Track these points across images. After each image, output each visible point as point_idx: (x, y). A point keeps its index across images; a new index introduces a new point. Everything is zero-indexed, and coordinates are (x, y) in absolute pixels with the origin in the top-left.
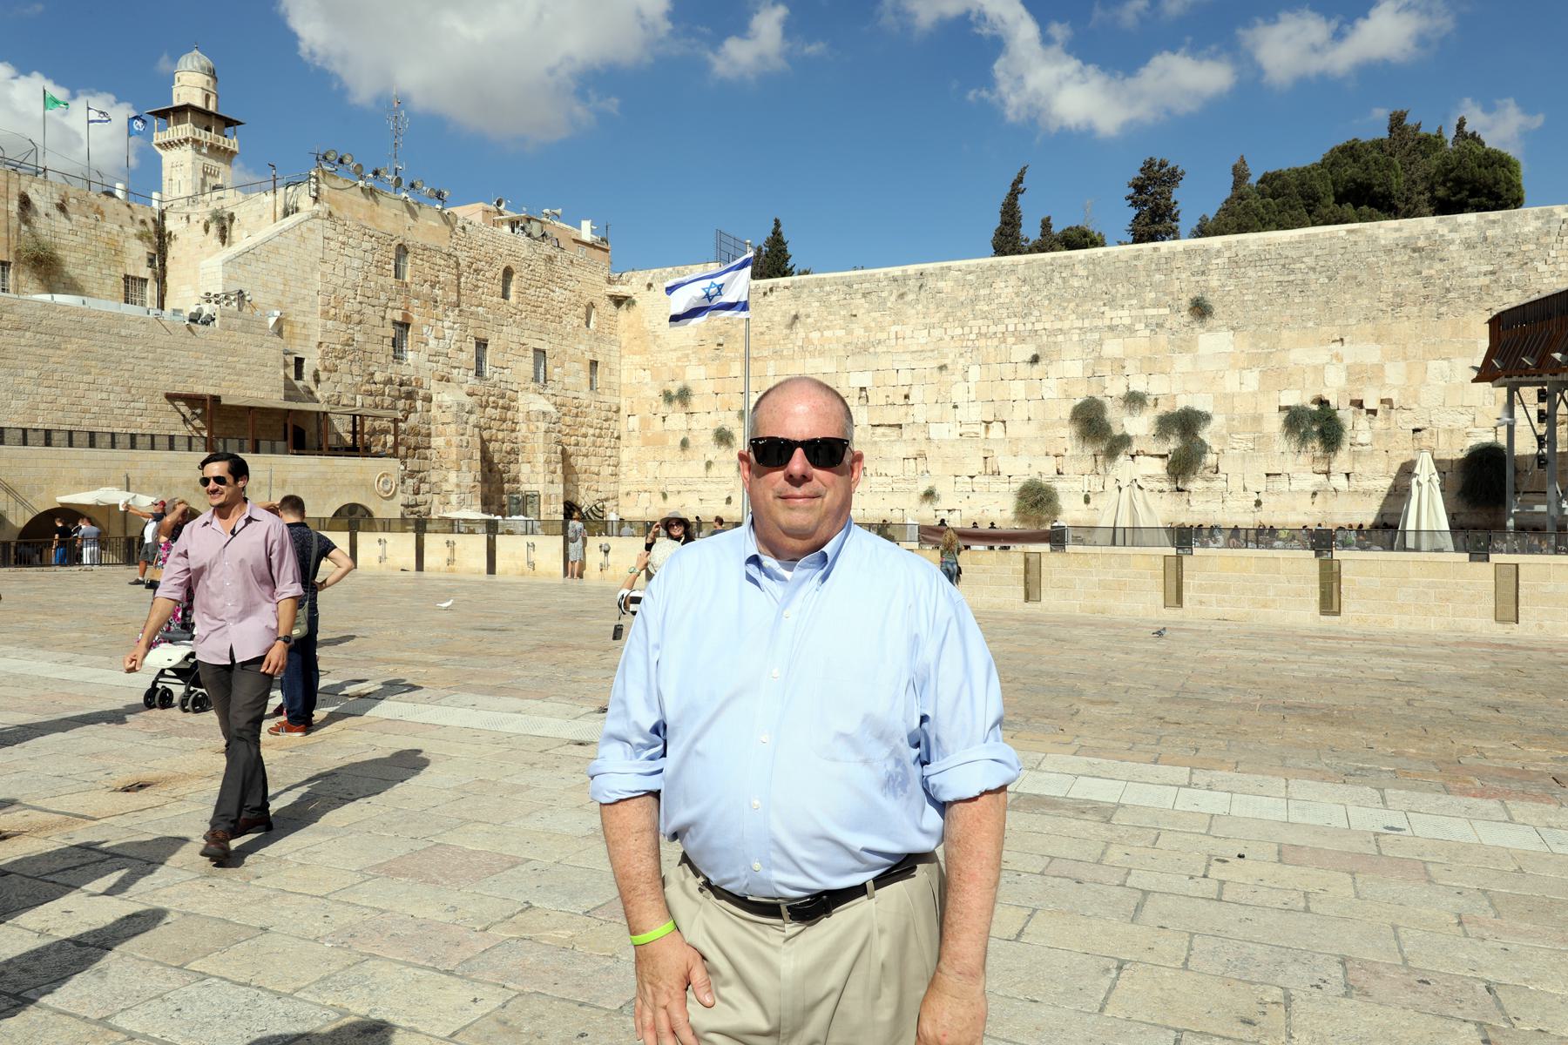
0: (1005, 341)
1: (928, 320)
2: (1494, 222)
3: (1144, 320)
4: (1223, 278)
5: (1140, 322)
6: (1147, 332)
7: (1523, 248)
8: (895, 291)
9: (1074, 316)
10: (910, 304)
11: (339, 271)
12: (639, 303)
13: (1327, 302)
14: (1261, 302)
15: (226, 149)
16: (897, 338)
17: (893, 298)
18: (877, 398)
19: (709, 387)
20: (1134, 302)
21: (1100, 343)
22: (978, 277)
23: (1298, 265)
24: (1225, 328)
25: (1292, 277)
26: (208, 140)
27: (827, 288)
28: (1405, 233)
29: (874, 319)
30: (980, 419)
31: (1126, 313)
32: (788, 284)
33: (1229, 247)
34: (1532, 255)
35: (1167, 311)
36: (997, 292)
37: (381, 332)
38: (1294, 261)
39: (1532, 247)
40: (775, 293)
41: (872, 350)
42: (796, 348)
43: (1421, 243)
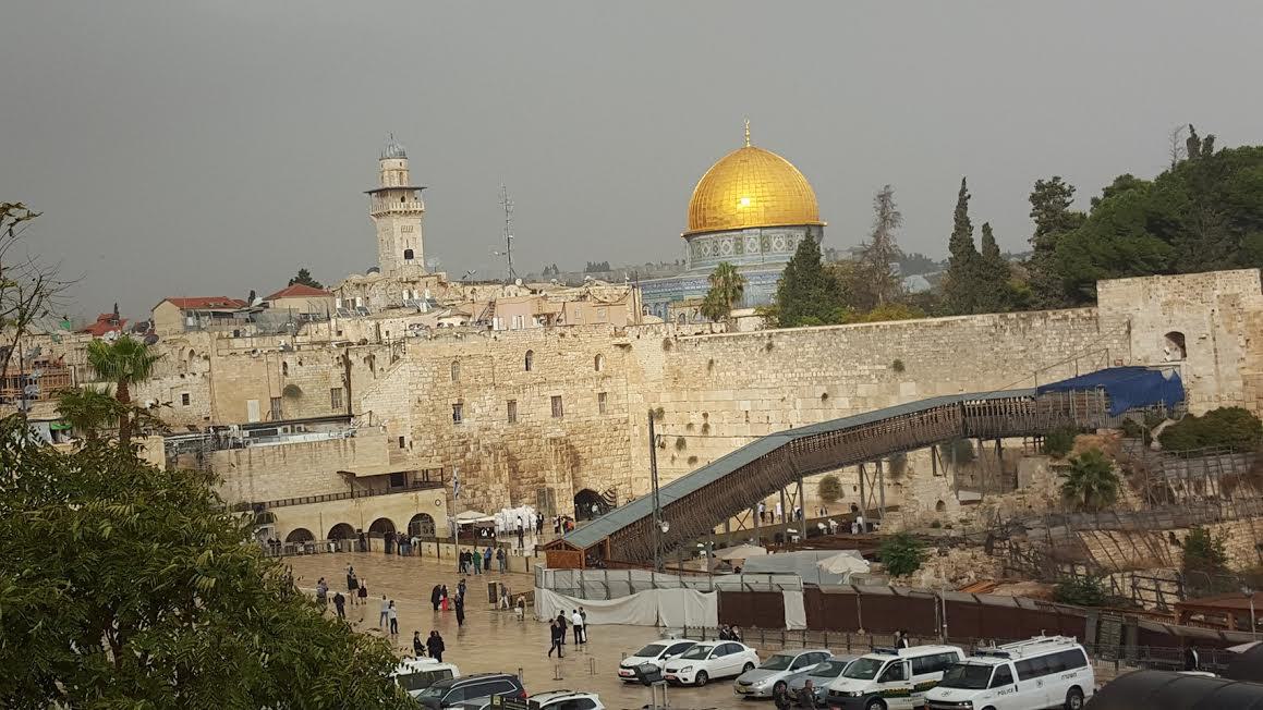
6: (876, 381)
11: (420, 386)
12: (634, 348)
15: (415, 211)
26: (403, 209)
31: (866, 367)
35: (884, 367)
37: (445, 413)
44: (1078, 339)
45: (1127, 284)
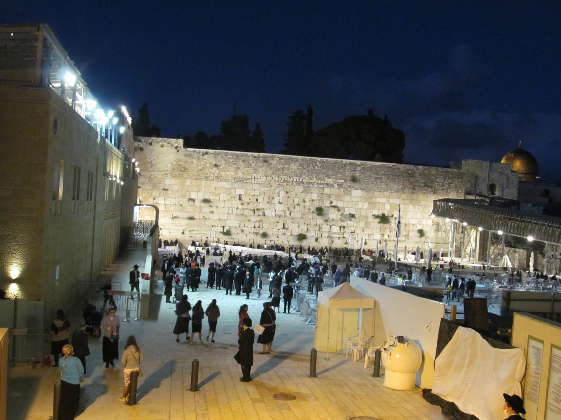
0: (292, 184)
1: (266, 174)
2: (426, 169)
3: (337, 183)
4: (360, 173)
5: (336, 184)
7: (432, 177)
8: (255, 161)
9: (316, 179)
10: (260, 167)
13: (387, 185)
14: (370, 182)
16: (255, 178)
17: (254, 164)
18: (245, 199)
19: (176, 188)
20: (334, 177)
21: (323, 188)
22: (285, 161)
23: (380, 173)
24: (360, 189)
25: (378, 176)
27: (229, 157)
28: (407, 168)
29: (246, 170)
30: (283, 210)
32: (213, 152)
33: (362, 164)
34: (434, 179)
35: (343, 181)
36: (291, 167)
38: (379, 172)
39: (434, 177)
40: (207, 155)
41: (245, 181)
42: (215, 177)
43: (410, 172)
44: (453, 181)
45: (477, 162)
